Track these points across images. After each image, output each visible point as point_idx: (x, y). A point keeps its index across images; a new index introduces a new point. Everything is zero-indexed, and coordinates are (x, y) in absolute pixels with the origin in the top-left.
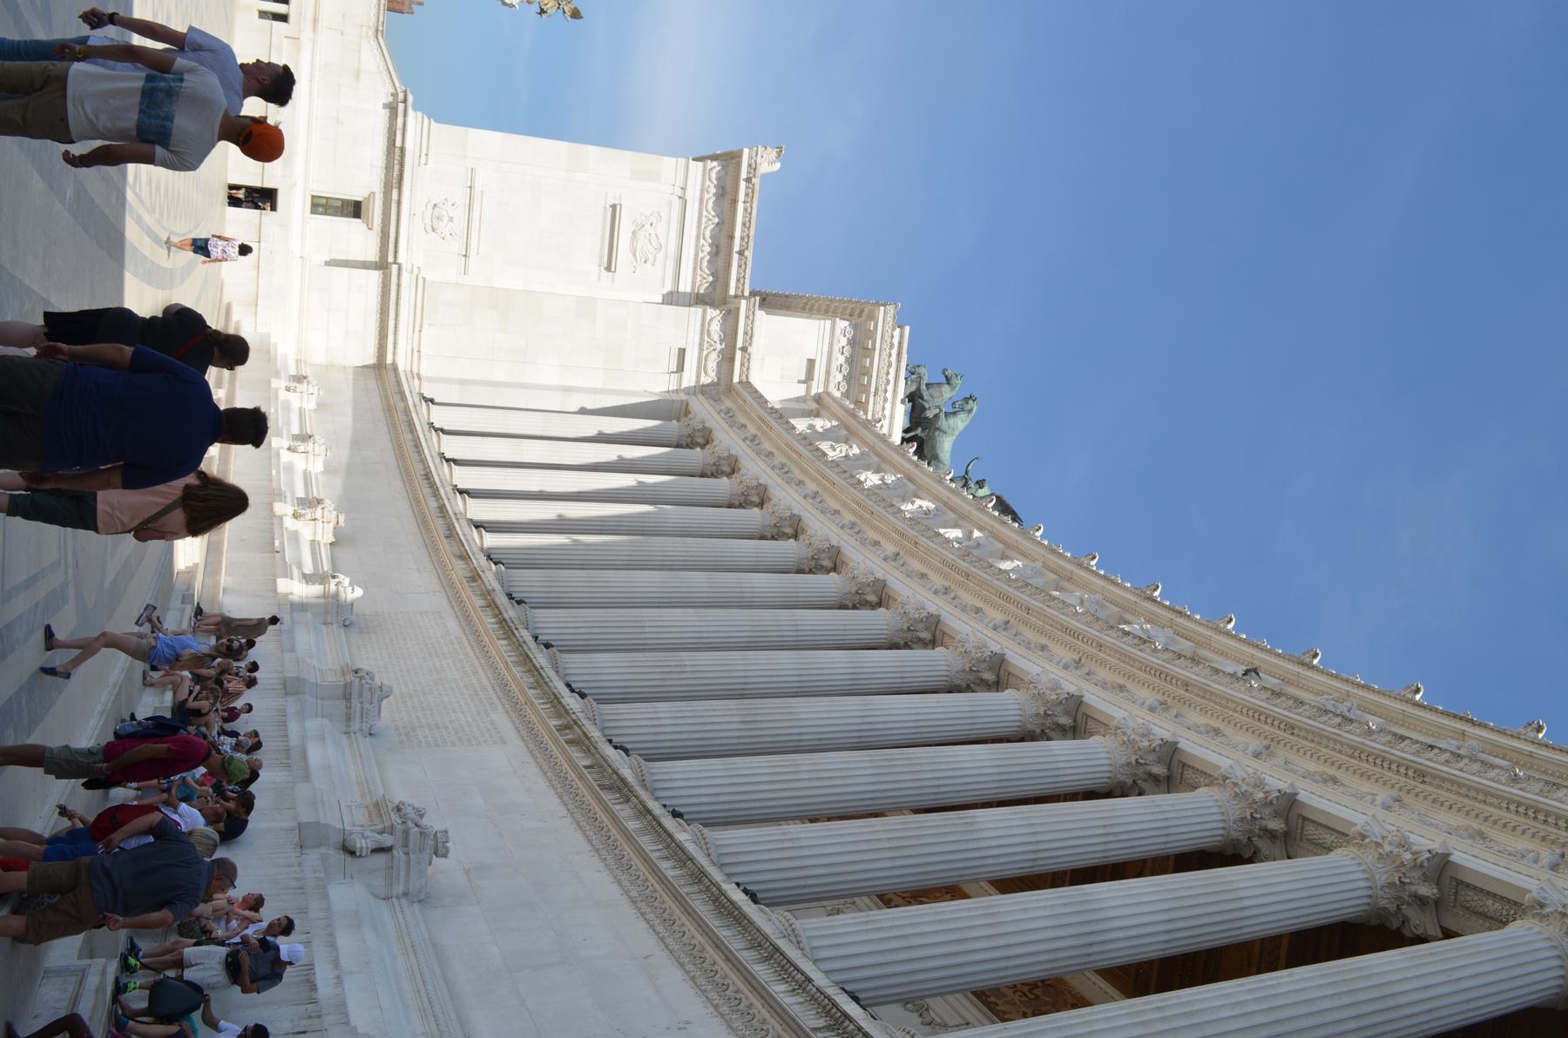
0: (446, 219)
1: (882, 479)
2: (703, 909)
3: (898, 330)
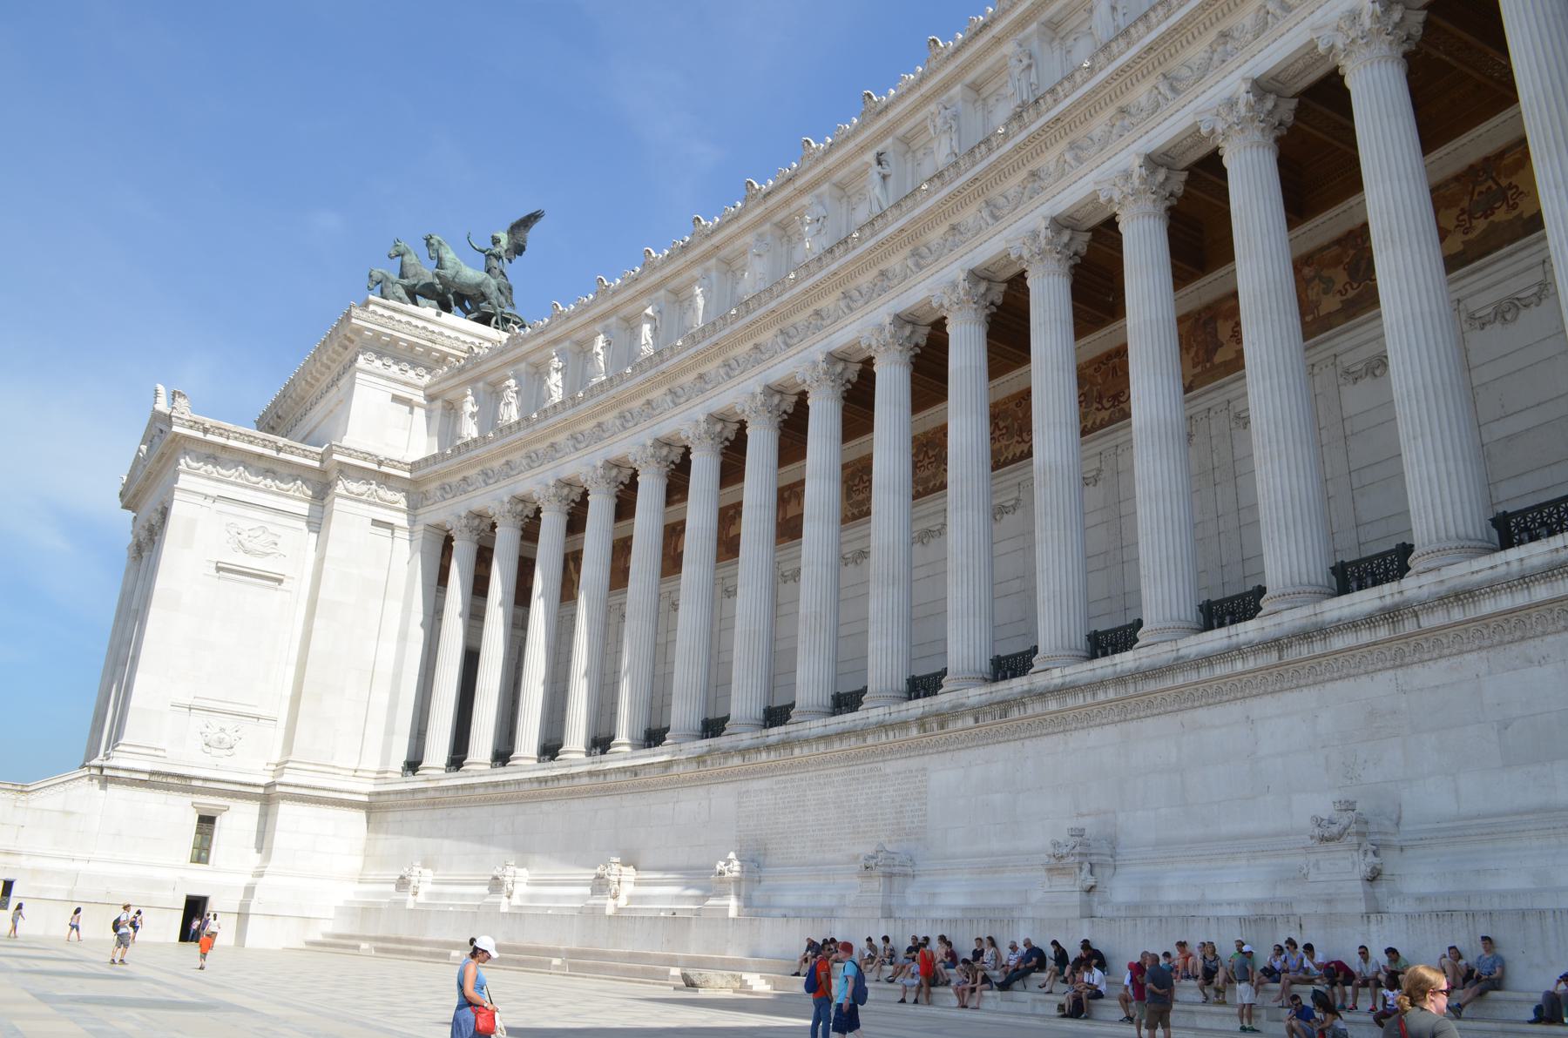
0: (222, 735)
1: (557, 370)
2: (1152, 686)
3: (372, 307)
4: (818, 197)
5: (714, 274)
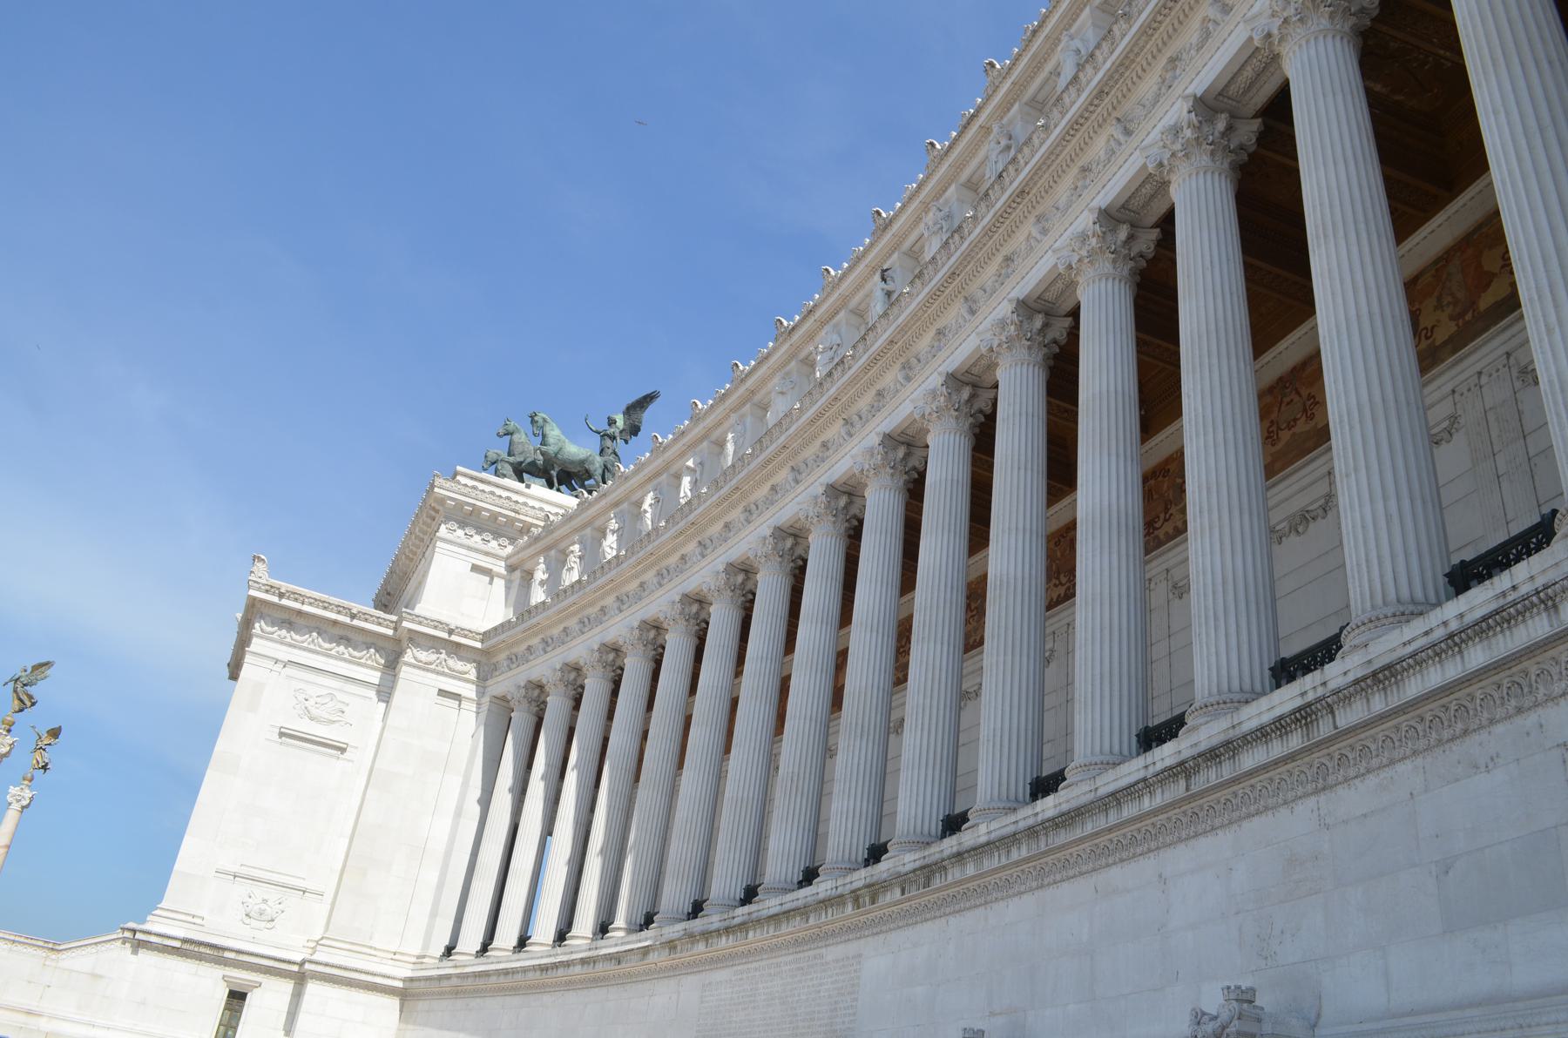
0: (263, 906)
1: (613, 532)
2: (1063, 837)
4: (835, 326)
5: (749, 420)
